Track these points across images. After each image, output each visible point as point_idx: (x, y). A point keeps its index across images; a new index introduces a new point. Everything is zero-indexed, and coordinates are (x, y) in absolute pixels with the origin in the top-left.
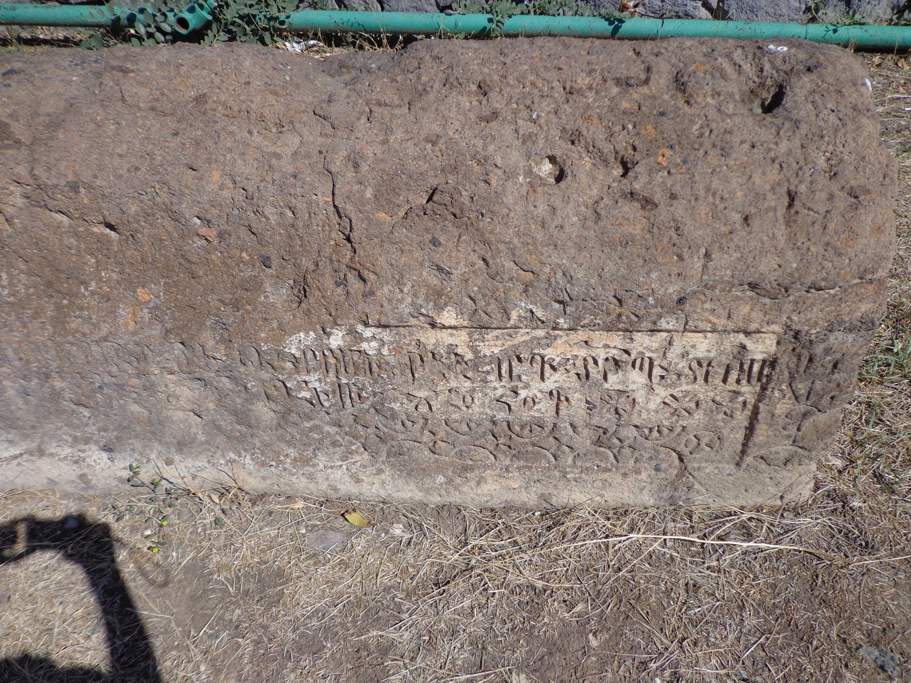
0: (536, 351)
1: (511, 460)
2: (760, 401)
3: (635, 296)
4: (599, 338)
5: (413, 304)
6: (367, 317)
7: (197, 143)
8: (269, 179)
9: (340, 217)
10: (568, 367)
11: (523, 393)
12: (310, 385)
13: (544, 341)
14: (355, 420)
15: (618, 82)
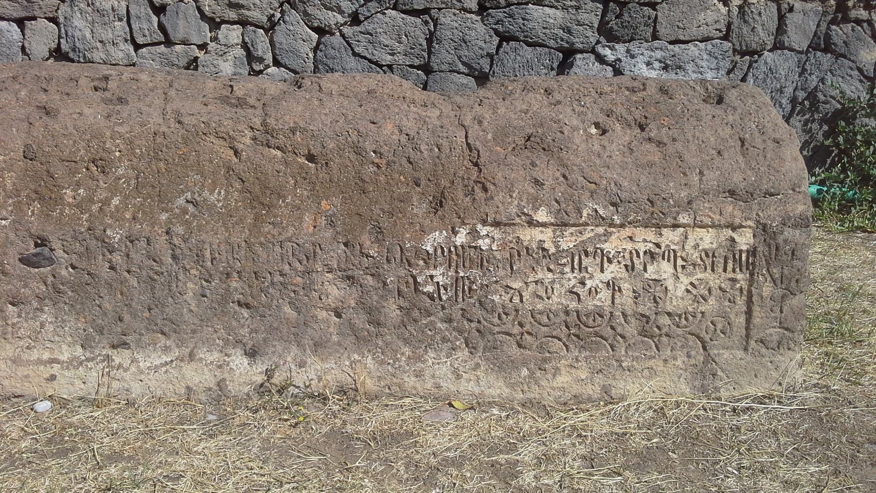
0: (598, 246)
1: (580, 352)
2: (751, 286)
3: (661, 199)
4: (641, 233)
5: (519, 205)
6: (487, 215)
7: (375, 110)
8: (425, 128)
9: (471, 151)
10: (620, 259)
11: (589, 283)
12: (435, 280)
13: (603, 238)
14: (462, 315)
15: (628, 89)
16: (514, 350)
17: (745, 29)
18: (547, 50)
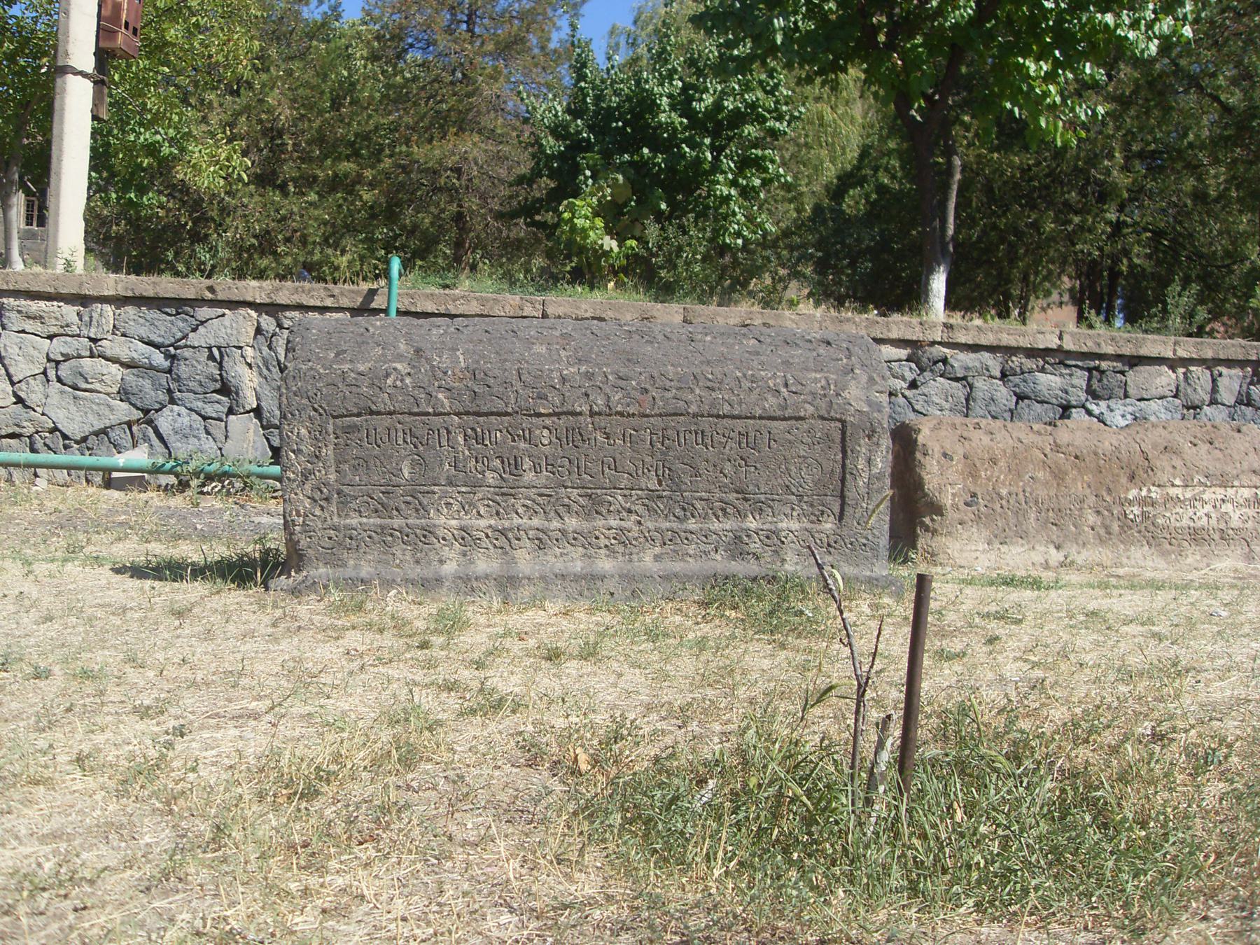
4: (1219, 490)
16: (1168, 547)
17: (1189, 390)
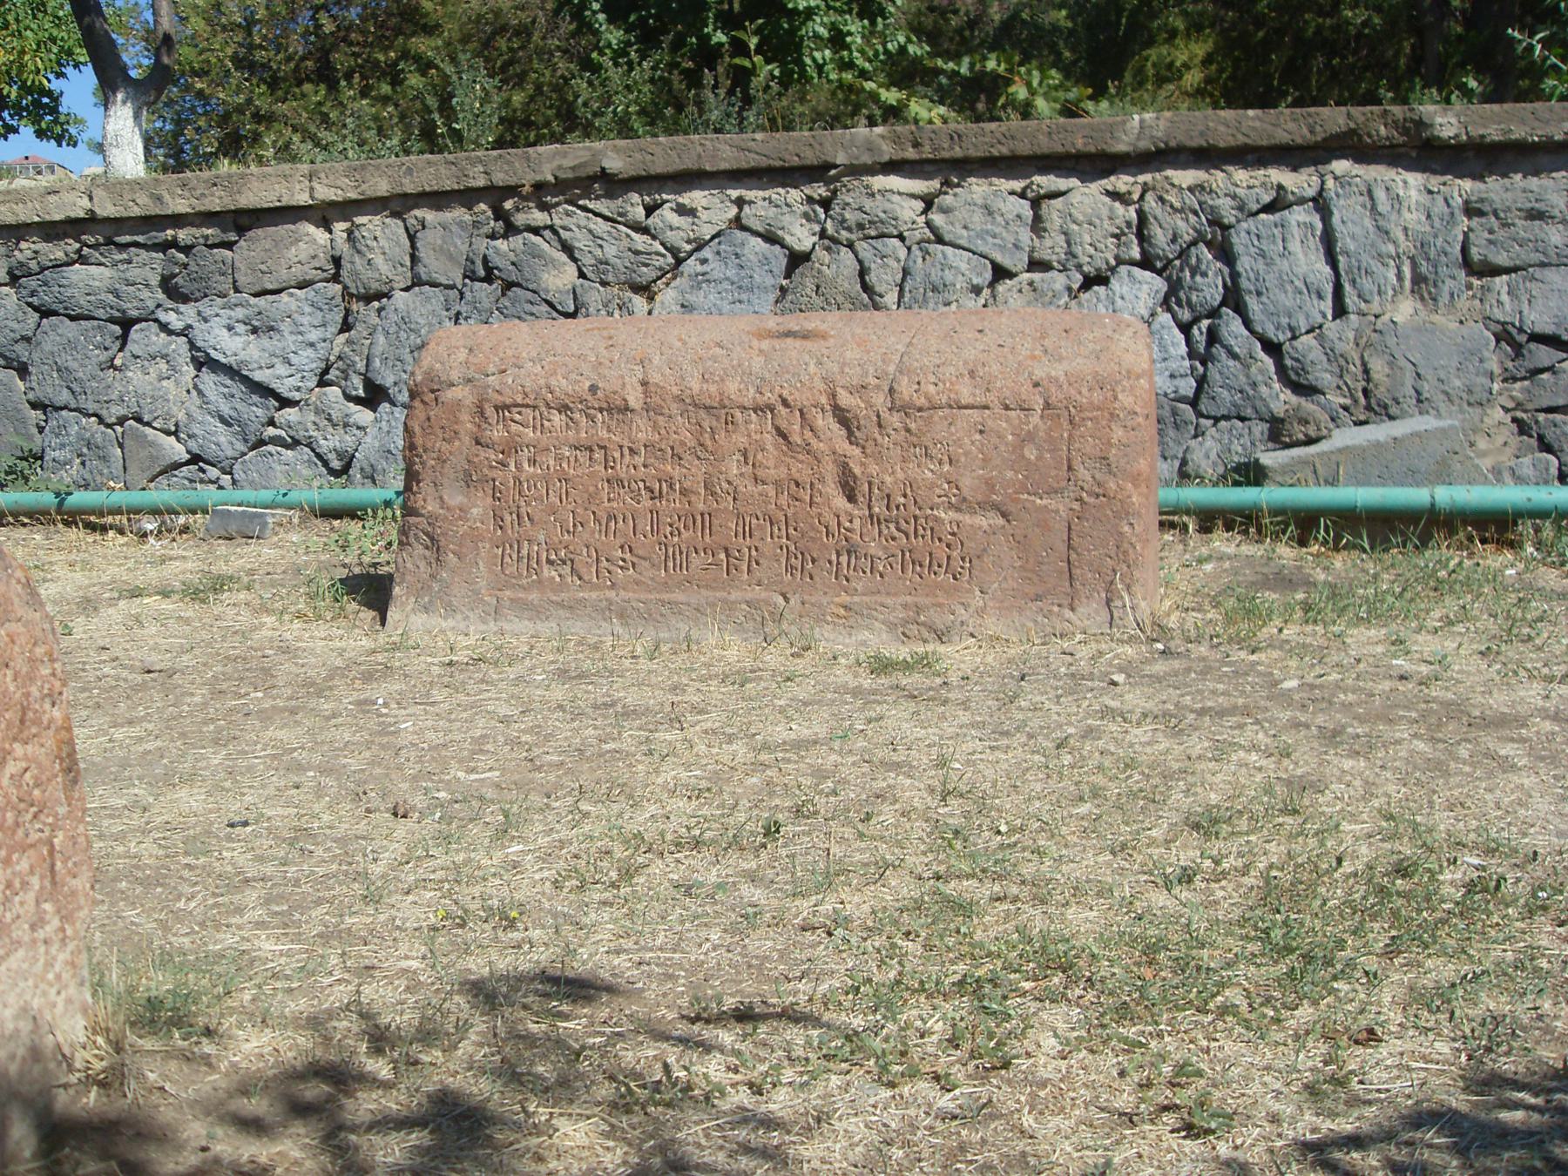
18: (95, 323)
